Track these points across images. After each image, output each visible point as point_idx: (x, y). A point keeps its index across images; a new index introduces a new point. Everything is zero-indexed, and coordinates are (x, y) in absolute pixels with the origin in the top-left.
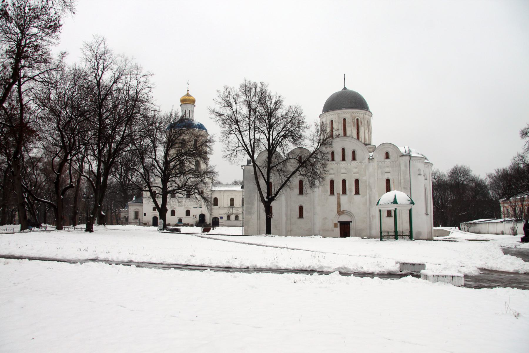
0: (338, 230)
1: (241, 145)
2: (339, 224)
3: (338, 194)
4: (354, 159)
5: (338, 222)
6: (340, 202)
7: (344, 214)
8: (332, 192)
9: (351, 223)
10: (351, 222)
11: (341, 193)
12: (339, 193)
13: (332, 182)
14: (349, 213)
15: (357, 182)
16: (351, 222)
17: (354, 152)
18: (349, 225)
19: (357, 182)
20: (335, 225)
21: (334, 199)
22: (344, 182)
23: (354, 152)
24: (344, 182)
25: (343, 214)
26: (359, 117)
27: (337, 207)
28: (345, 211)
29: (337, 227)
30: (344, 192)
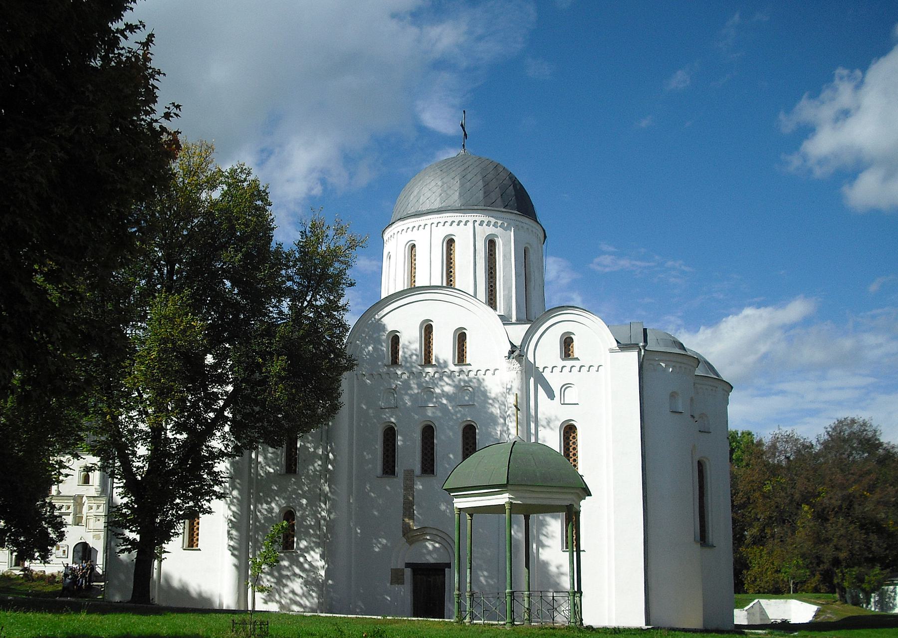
0: (405, 591)
2: (408, 572)
3: (409, 475)
4: (461, 357)
5: (408, 565)
8: (389, 468)
12: (413, 471)
13: (390, 434)
17: (461, 338)
20: (397, 577)
21: (394, 487)
22: (428, 432)
23: (461, 338)
24: (428, 432)
29: (403, 583)
30: (428, 466)
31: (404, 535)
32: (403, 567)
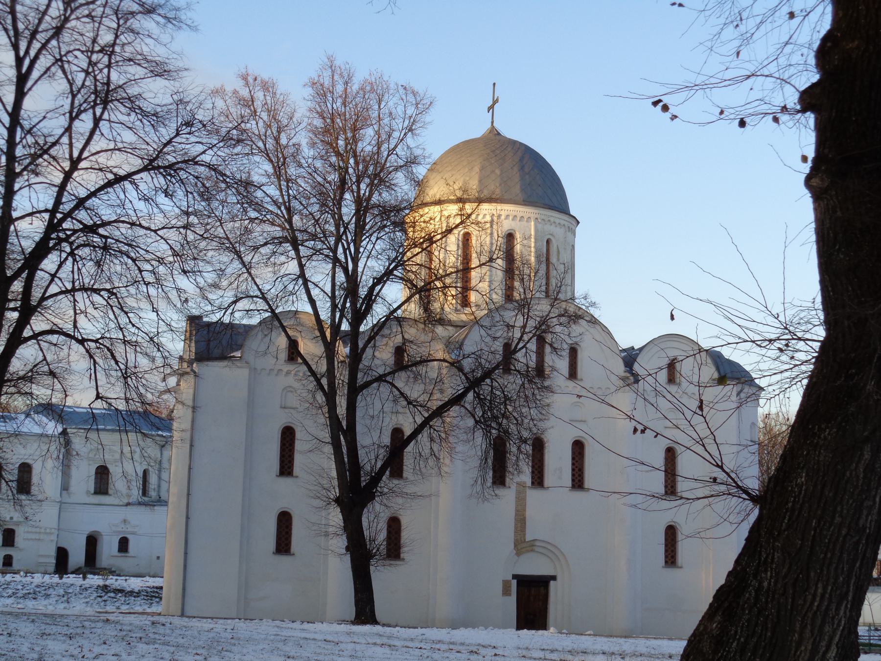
1: (258, 293)
2: (514, 583)
5: (515, 577)
6: (525, 510)
7: (532, 551)
9: (552, 583)
10: (554, 578)
11: (529, 483)
14: (551, 551)
15: (578, 448)
16: (554, 578)
18: (542, 590)
19: (578, 448)
25: (528, 551)
26: (551, 235)
27: (516, 528)
28: (537, 543)
29: (510, 595)
30: (538, 480)
31: (516, 546)
32: (511, 578)
